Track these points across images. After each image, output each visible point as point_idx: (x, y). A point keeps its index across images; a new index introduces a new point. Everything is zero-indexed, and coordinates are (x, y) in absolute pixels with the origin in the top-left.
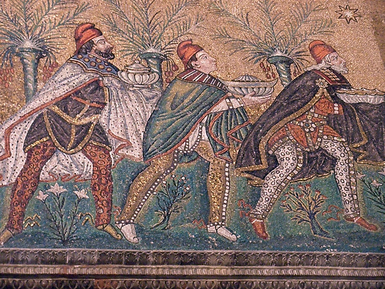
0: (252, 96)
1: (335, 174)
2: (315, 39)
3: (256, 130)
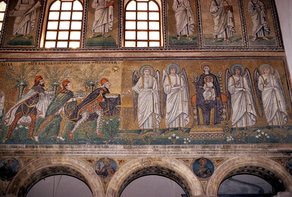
1: (97, 120)
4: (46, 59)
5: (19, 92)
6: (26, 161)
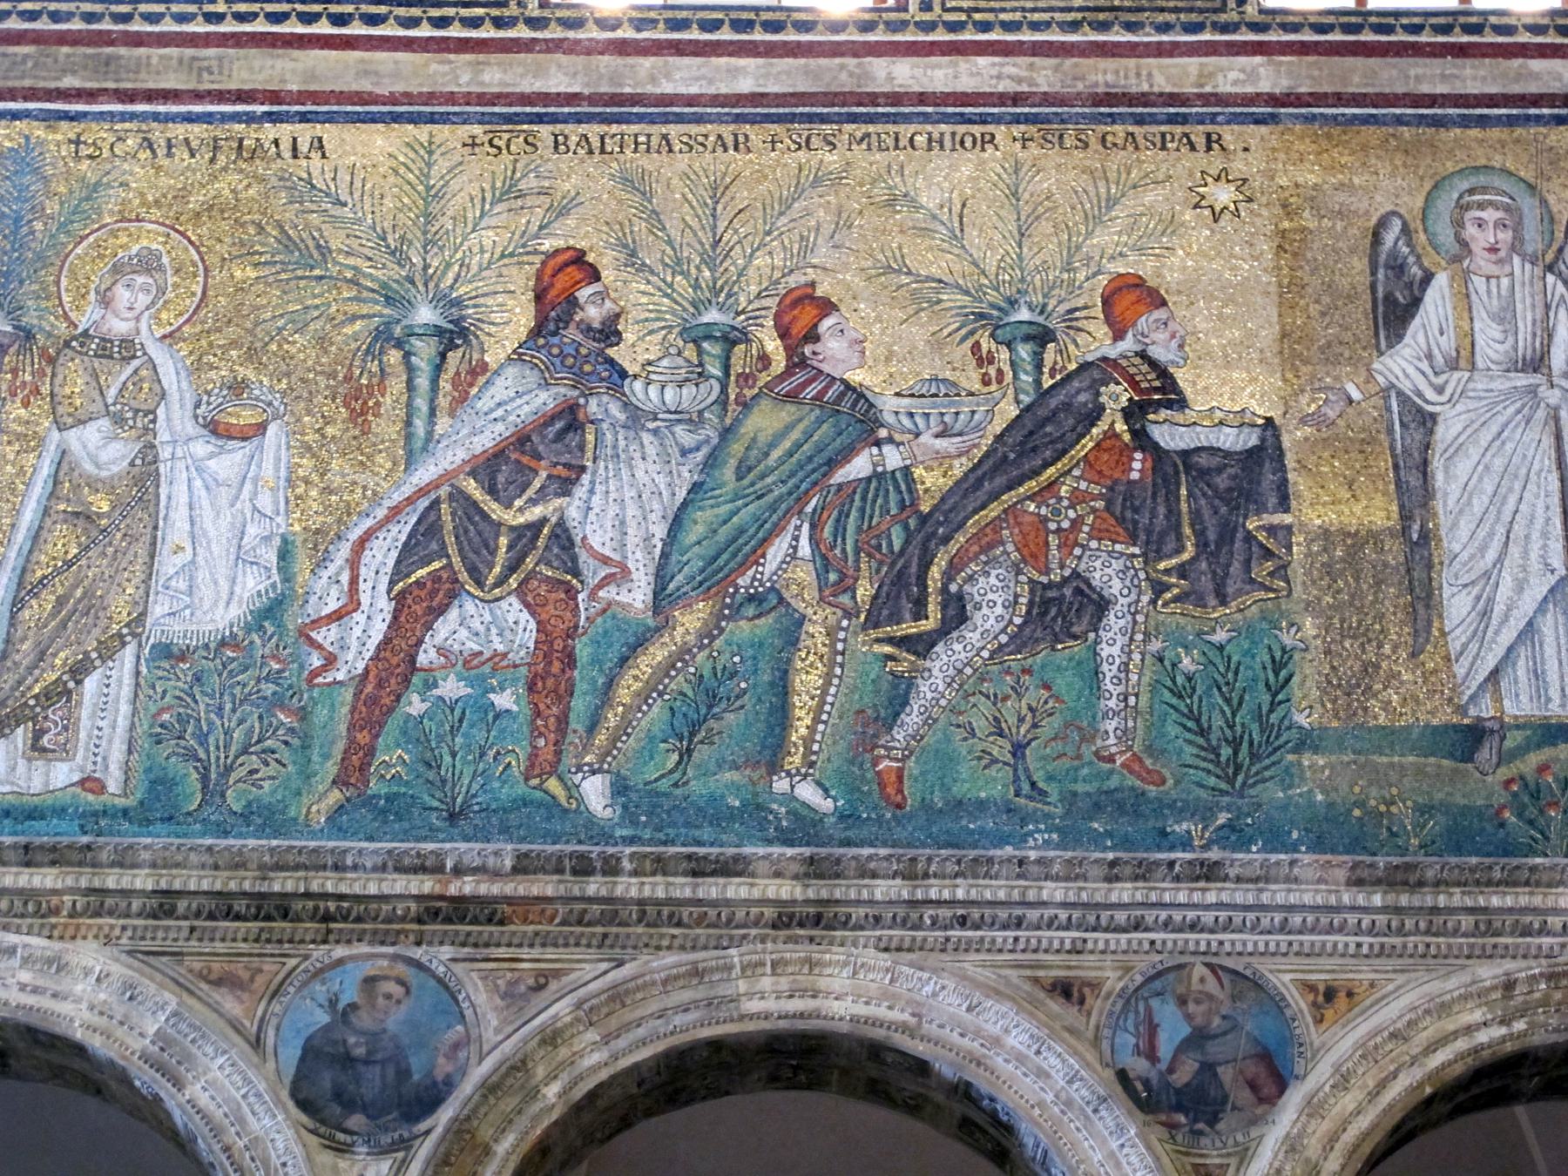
0: (937, 436)
1: (1096, 643)
2: (1122, 271)
3: (930, 530)
4: (615, 107)
5: (410, 386)
6: (523, 988)
